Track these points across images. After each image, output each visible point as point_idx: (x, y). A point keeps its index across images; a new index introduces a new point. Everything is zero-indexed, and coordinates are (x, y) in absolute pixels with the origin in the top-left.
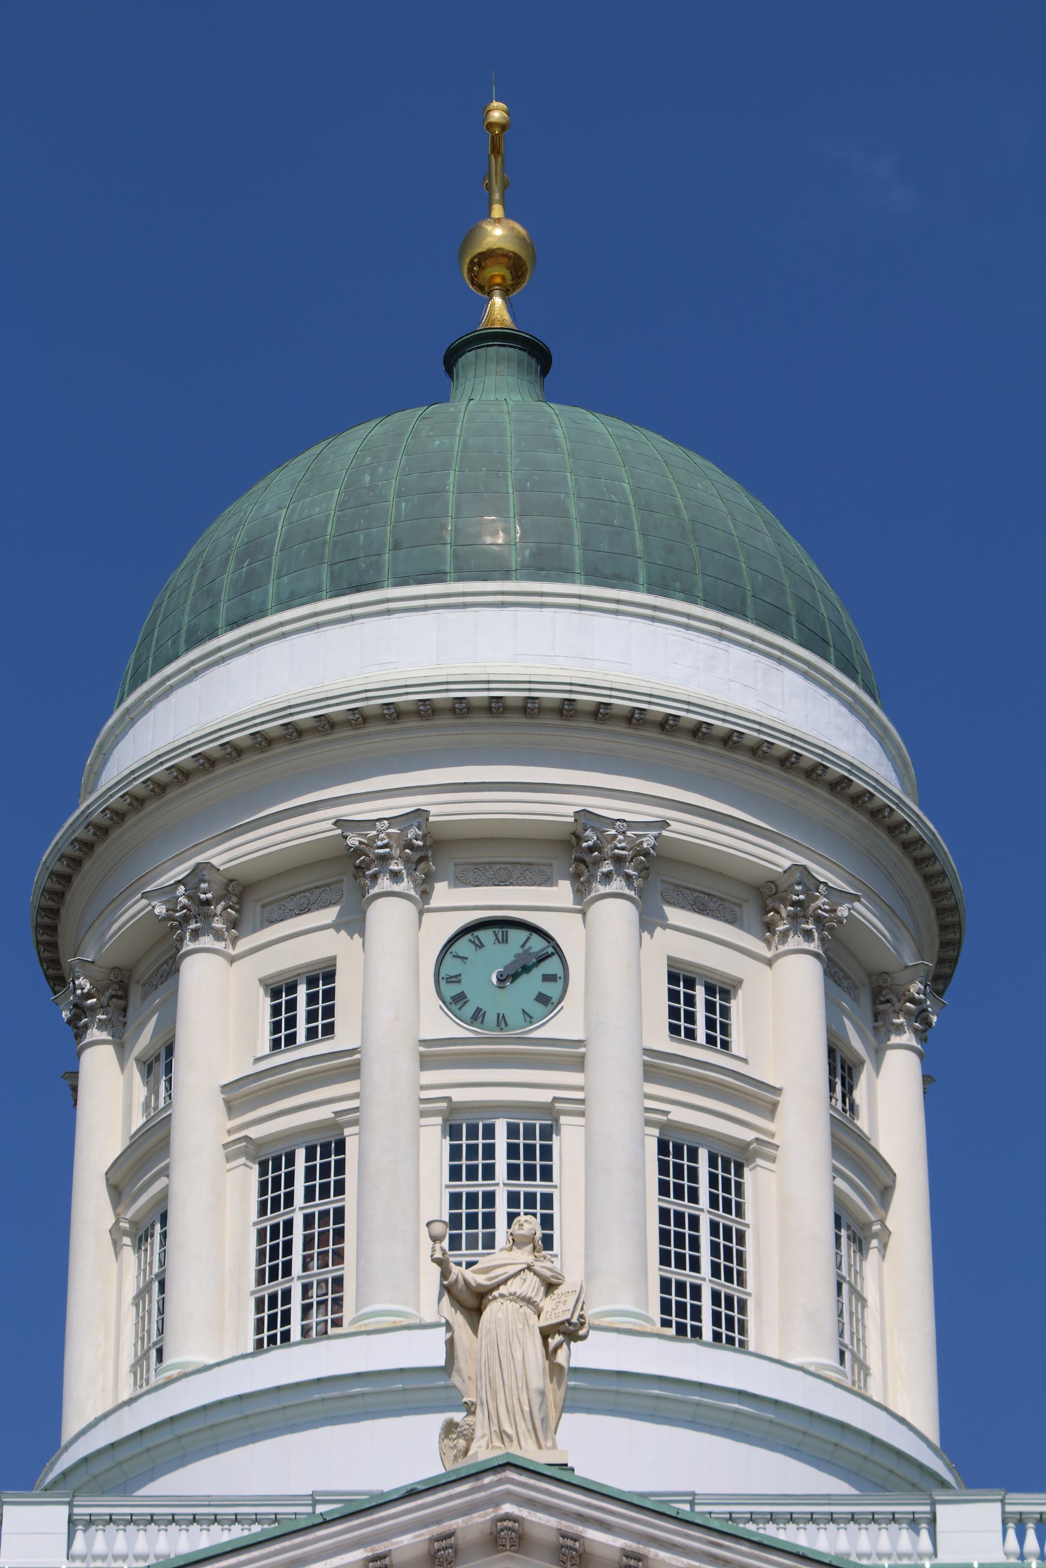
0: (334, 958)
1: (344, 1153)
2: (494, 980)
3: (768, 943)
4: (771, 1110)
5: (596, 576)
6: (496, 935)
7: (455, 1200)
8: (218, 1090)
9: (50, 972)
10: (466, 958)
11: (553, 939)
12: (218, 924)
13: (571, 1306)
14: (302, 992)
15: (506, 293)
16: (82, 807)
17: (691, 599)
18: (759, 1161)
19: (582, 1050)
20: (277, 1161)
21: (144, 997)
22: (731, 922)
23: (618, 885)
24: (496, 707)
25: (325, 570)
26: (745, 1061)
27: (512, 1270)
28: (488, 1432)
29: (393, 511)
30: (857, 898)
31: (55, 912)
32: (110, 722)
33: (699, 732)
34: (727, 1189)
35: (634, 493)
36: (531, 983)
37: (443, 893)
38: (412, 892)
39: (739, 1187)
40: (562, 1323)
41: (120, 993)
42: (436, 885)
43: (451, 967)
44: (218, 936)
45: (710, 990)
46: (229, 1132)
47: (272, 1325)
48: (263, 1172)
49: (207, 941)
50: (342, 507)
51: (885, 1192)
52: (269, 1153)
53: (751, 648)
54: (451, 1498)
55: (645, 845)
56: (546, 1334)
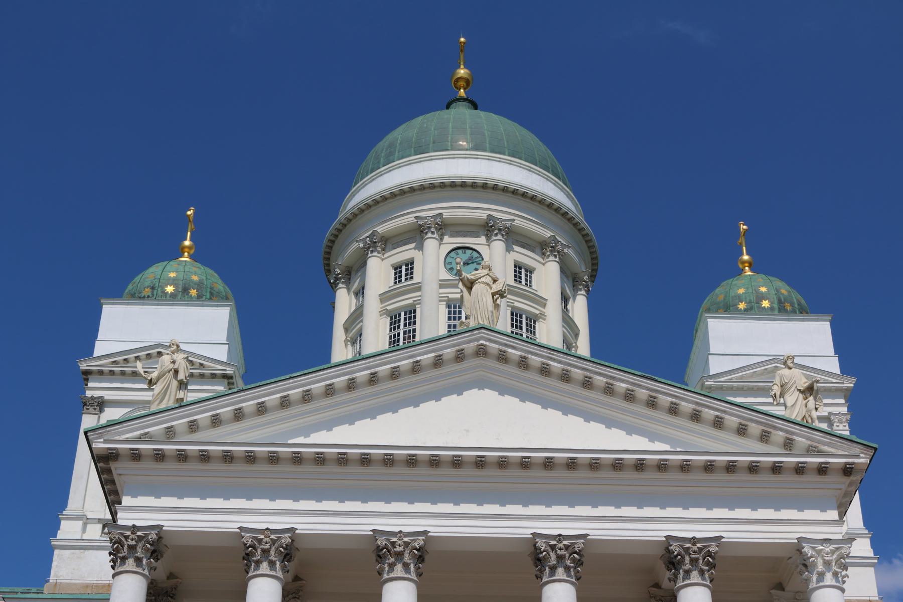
1: (415, 318)
3: (543, 259)
4: (544, 306)
5: (492, 151)
7: (449, 326)
8: (378, 296)
13: (502, 286)
14: (404, 268)
15: (465, 89)
16: (338, 219)
17: (520, 159)
18: (540, 320)
21: (356, 274)
22: (533, 251)
23: (499, 237)
24: (463, 185)
25: (413, 149)
26: (536, 291)
27: (482, 275)
31: (329, 253)
32: (347, 197)
33: (524, 195)
34: (531, 327)
36: (474, 266)
37: (447, 239)
39: (534, 327)
40: (499, 291)
41: (348, 274)
43: (449, 260)
44: (379, 252)
45: (526, 270)
46: (381, 308)
49: (375, 254)
51: (577, 335)
52: (393, 314)
53: (539, 175)
54: (463, 338)
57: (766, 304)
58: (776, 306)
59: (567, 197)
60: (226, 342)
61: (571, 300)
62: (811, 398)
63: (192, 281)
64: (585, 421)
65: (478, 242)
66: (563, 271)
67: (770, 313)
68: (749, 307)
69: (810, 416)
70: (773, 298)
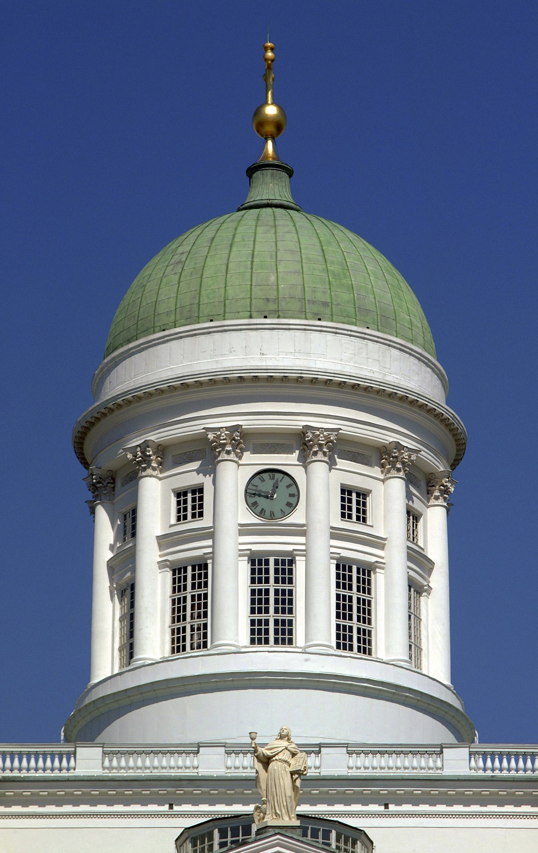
0: (203, 483)
6: (270, 476)
10: (257, 486)
12: (154, 465)
14: (190, 496)
18: (378, 570)
19: (305, 528)
20: (180, 570)
27: (280, 749)
28: (271, 812)
37: (248, 457)
39: (369, 581)
40: (298, 770)
41: (112, 481)
44: (154, 469)
45: (358, 495)
48: (174, 574)
49: (149, 471)
55: (332, 439)
56: (292, 773)
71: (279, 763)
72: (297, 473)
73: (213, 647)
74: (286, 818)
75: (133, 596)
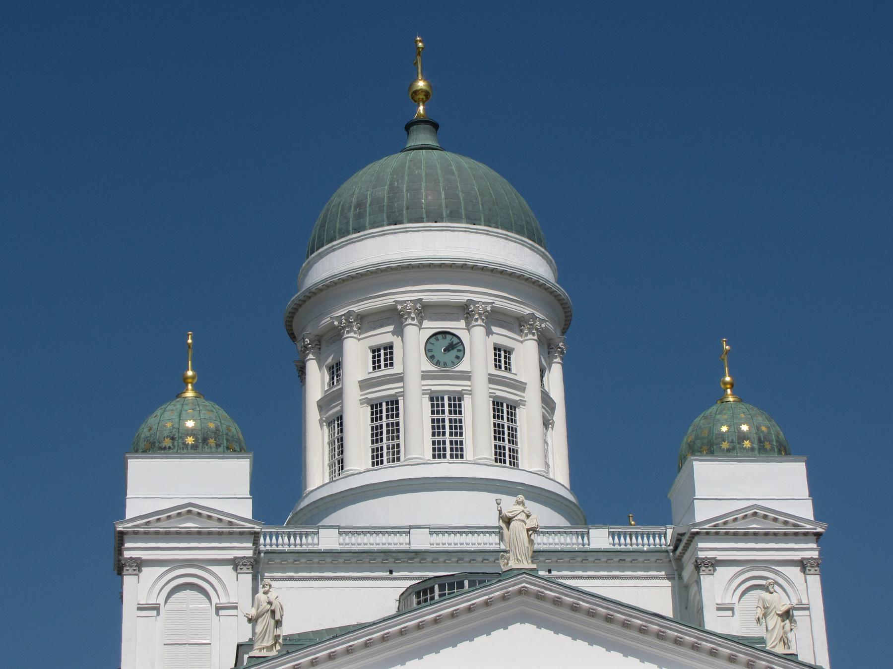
2: (443, 351)
3: (522, 338)
4: (523, 390)
9: (290, 332)
11: (460, 338)
12: (355, 329)
14: (382, 352)
15: (424, 103)
17: (497, 228)
18: (521, 406)
19: (470, 374)
22: (510, 330)
26: (516, 374)
27: (518, 512)
29: (405, 196)
30: (547, 321)
35: (479, 190)
36: (454, 353)
37: (426, 324)
38: (417, 324)
41: (318, 344)
42: (424, 321)
45: (505, 352)
46: (361, 395)
47: (377, 458)
48: (372, 408)
49: (352, 334)
50: (389, 193)
52: (374, 403)
56: (528, 530)
57: (747, 444)
58: (756, 446)
59: (543, 258)
60: (249, 496)
61: (547, 370)
62: (787, 621)
63: (209, 429)
64: (607, 650)
65: (457, 326)
66: (540, 342)
67: (750, 453)
68: (731, 447)
69: (786, 637)
70: (754, 438)
71: (519, 523)
72: (463, 335)
73: (406, 460)
74: (525, 562)
75: (341, 425)
